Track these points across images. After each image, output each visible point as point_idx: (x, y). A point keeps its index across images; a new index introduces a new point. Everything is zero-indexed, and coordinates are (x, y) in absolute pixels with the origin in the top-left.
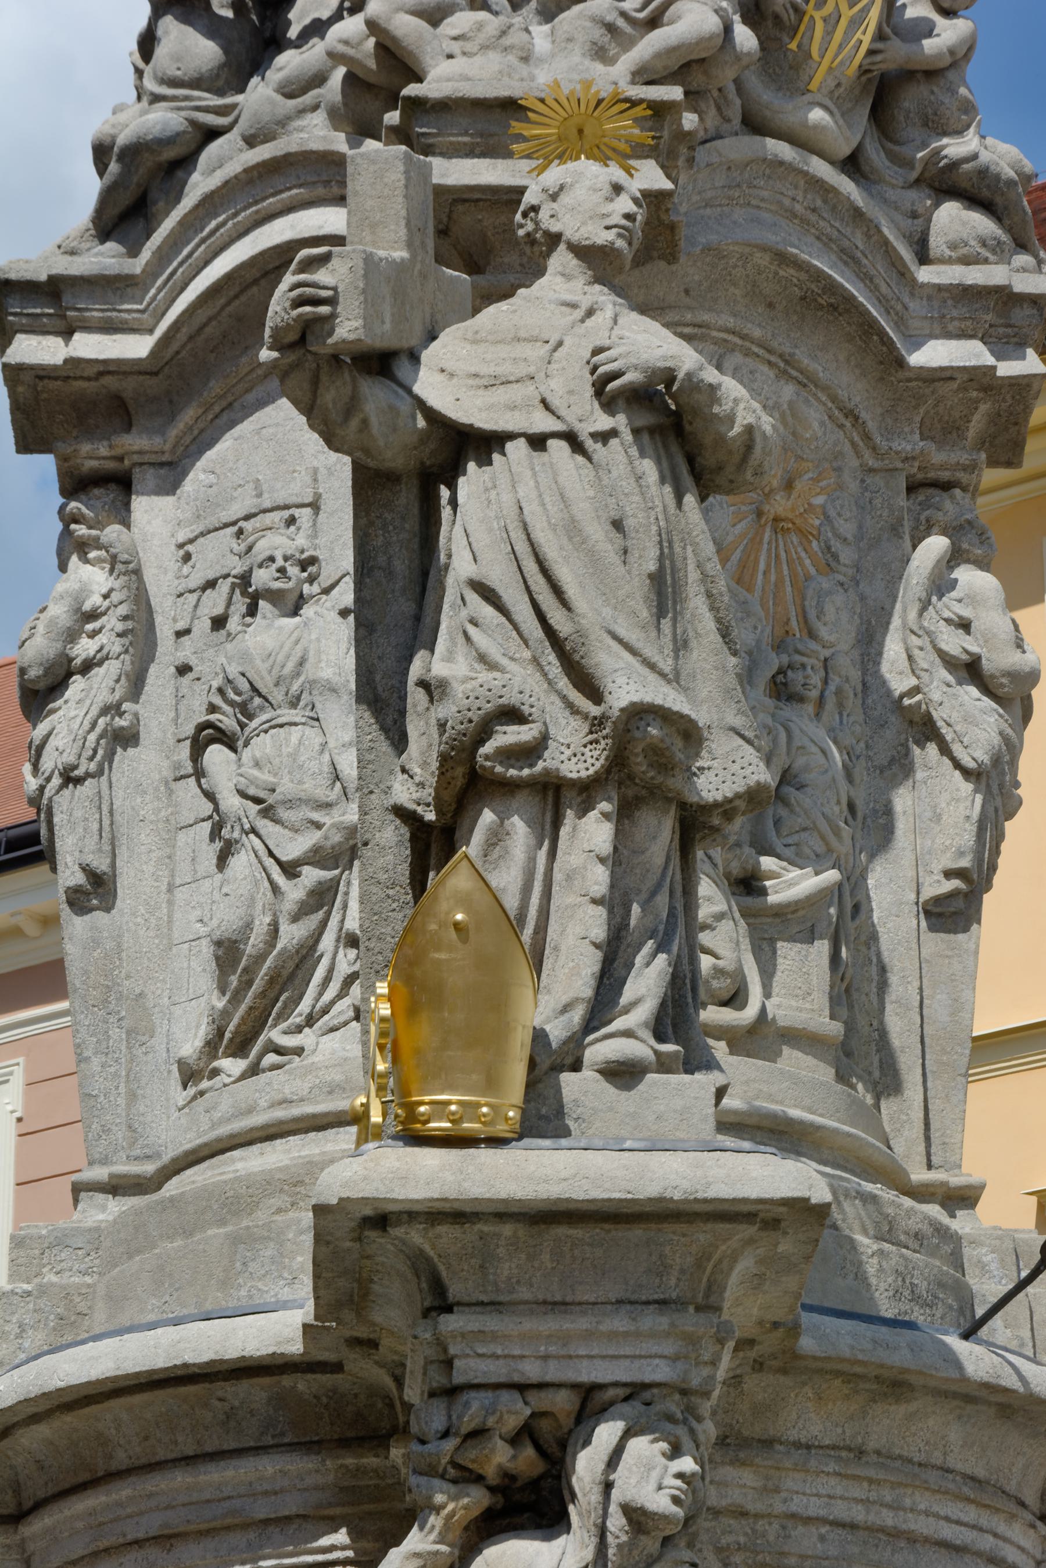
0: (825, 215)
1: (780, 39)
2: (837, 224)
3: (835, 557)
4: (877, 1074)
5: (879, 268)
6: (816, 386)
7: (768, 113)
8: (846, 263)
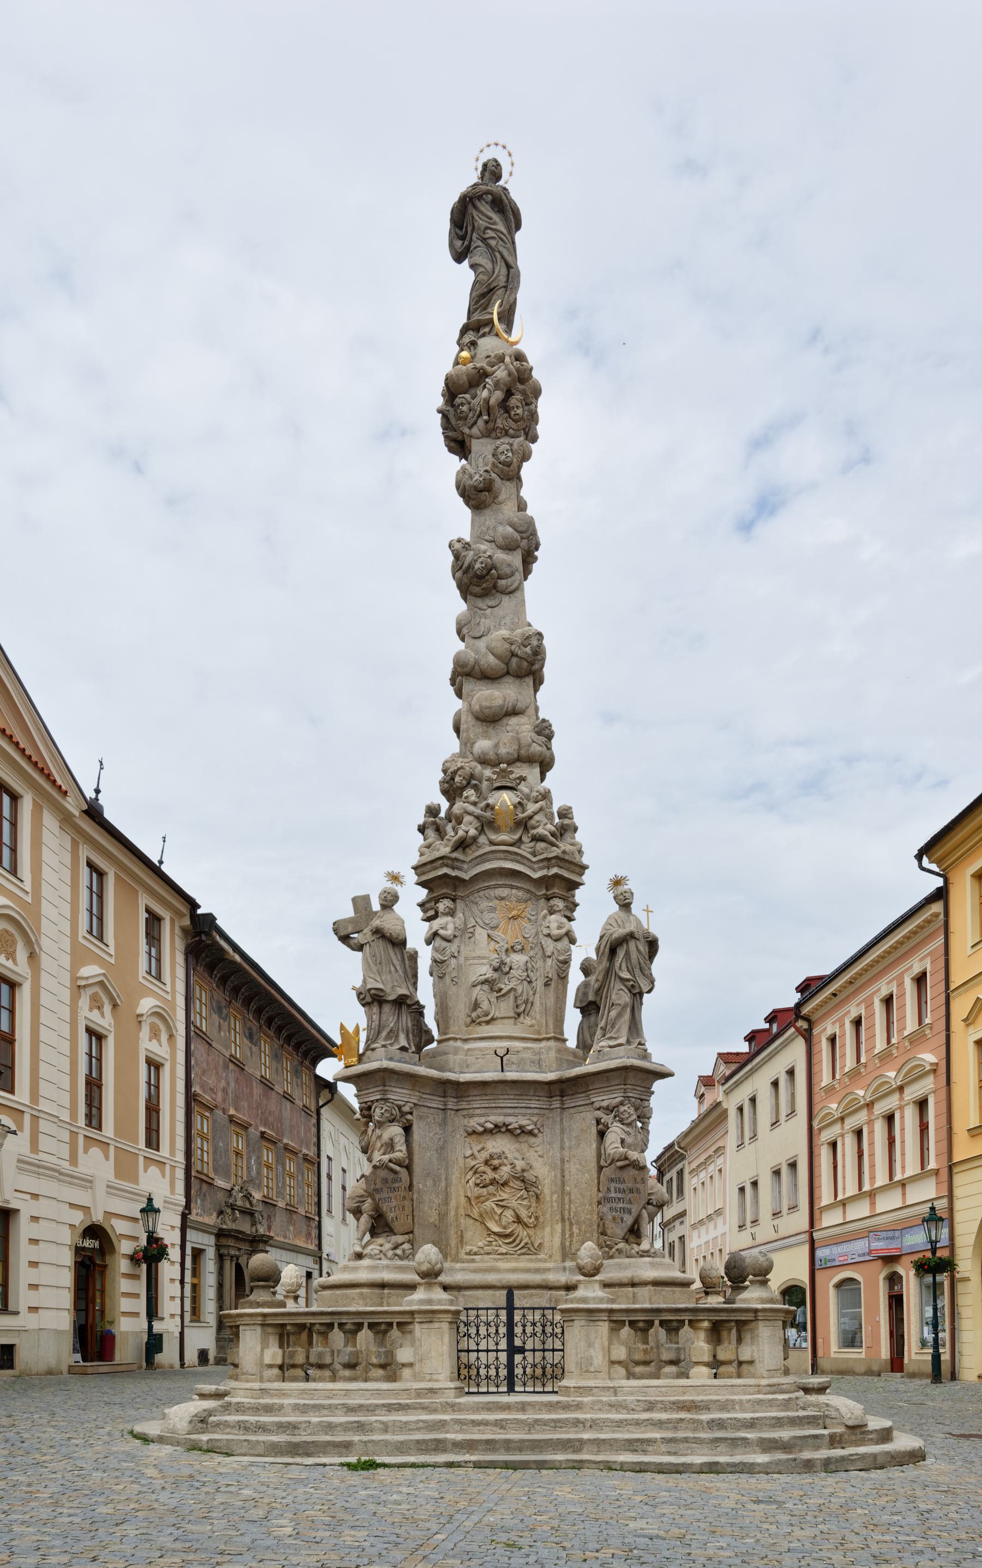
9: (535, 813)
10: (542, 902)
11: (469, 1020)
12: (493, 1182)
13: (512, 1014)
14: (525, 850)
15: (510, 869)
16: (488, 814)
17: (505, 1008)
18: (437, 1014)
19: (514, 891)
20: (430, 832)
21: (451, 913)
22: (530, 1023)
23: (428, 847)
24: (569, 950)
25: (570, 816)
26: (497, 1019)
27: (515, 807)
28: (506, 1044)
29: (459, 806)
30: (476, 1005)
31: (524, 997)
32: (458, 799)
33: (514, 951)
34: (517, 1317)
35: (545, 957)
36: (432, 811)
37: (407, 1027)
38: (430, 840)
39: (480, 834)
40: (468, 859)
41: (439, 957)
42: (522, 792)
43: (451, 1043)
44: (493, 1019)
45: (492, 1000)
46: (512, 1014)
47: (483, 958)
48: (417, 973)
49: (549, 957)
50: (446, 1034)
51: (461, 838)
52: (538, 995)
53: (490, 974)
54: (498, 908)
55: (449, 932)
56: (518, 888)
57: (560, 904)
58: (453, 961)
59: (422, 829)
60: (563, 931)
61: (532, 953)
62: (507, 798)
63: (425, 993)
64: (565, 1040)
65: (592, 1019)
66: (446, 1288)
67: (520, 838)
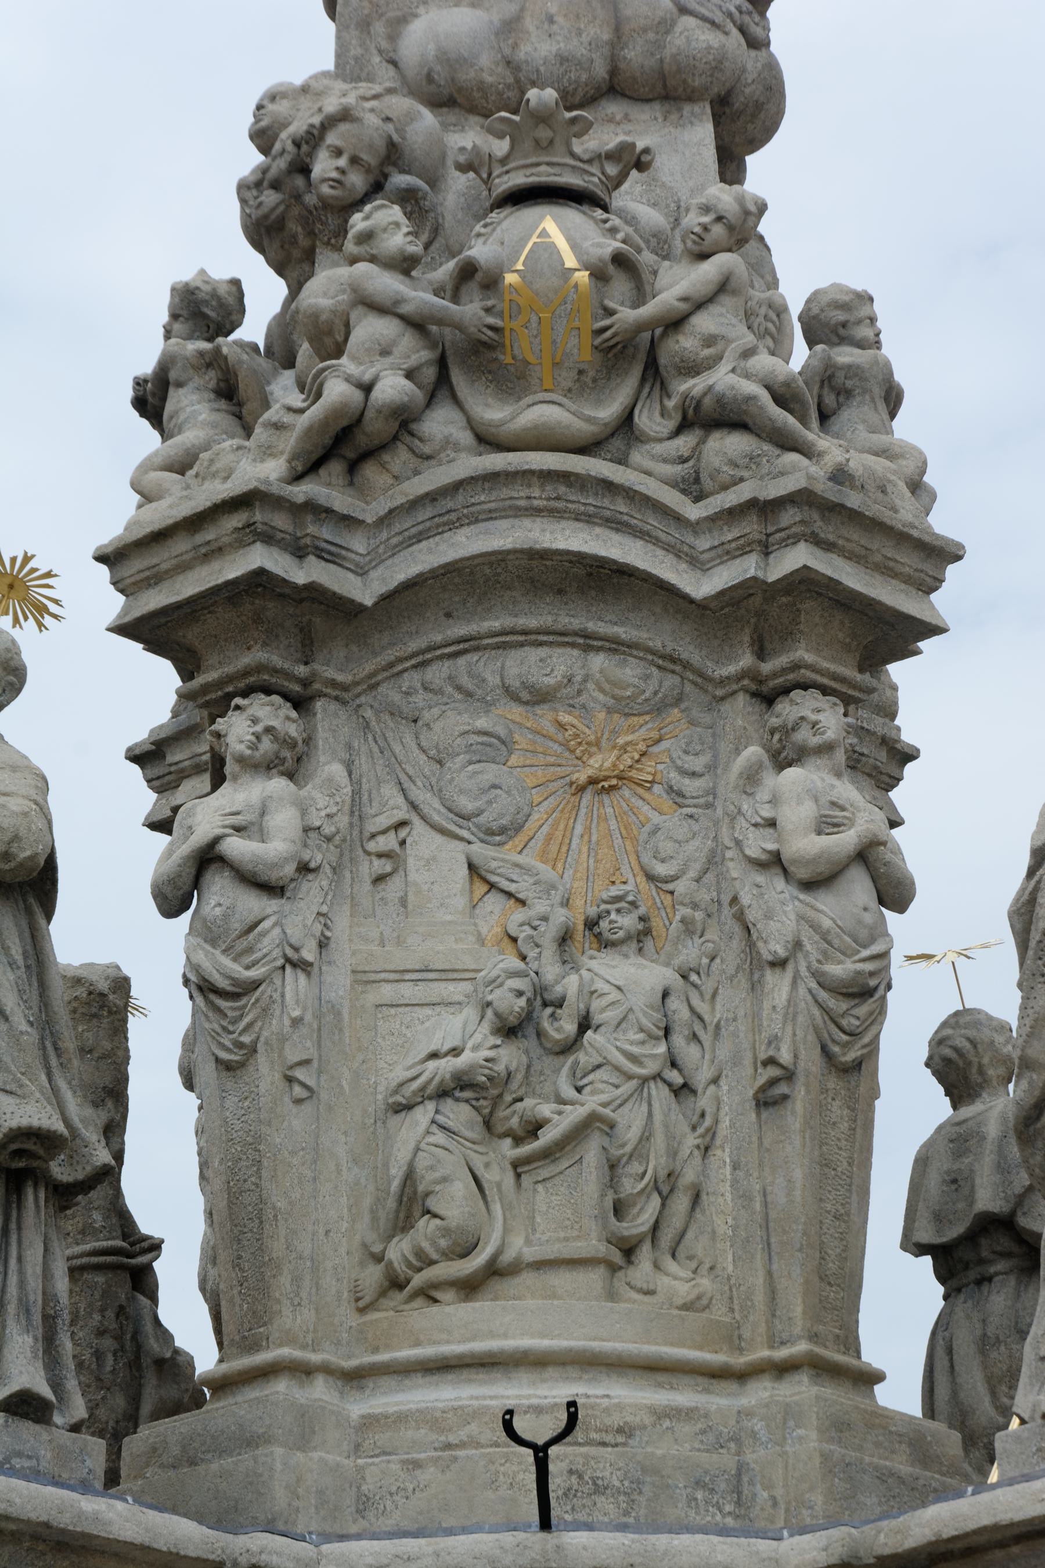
0: (574, 498)
1: (496, 359)
2: (590, 501)
3: (680, 794)
4: (730, 1268)
5: (653, 522)
6: (629, 647)
7: (493, 430)
8: (617, 530)
9: (700, 304)
10: (740, 711)
11: (373, 1276)
13: (593, 1245)
14: (649, 471)
15: (579, 558)
16: (471, 310)
17: (559, 1213)
18: (210, 1257)
19: (598, 661)
20: (194, 407)
21: (290, 762)
22: (684, 1291)
23: (181, 466)
24: (879, 931)
25: (864, 332)
26: (514, 1269)
27: (599, 275)
28: (557, 1391)
29: (328, 284)
30: (410, 1203)
31: (657, 1162)
32: (323, 255)
33: (605, 944)
35: (759, 965)
36: (204, 311)
37: (49, 1297)
38: (189, 437)
39: (430, 401)
40: (380, 507)
41: (224, 967)
42: (631, 220)
43: (281, 1387)
44: (494, 1271)
45: (490, 1177)
46: (593, 1245)
47: (448, 975)
48: (123, 1080)
49: (779, 964)
50: (252, 1346)
51: (337, 412)
52: (722, 1155)
53: (480, 1049)
54: (522, 740)
55: (273, 848)
56: (615, 646)
57: (830, 720)
58: (295, 984)
59: (151, 401)
60: (847, 840)
61: (690, 952)
62: (557, 235)
63: (163, 1181)
64: (869, 1378)
65: (999, 1299)
67: (627, 420)
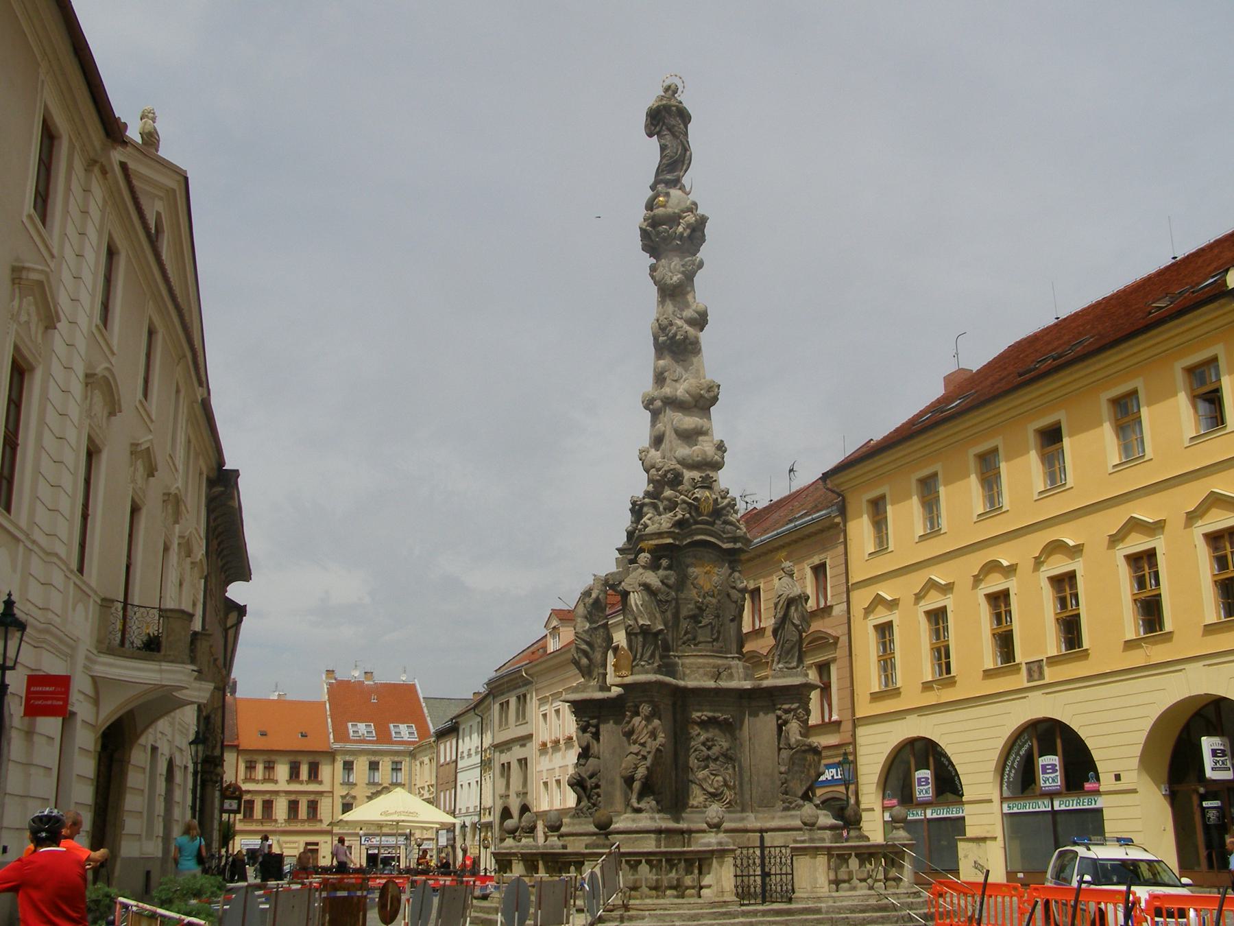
12: (708, 757)
34: (766, 852)
66: (726, 831)
